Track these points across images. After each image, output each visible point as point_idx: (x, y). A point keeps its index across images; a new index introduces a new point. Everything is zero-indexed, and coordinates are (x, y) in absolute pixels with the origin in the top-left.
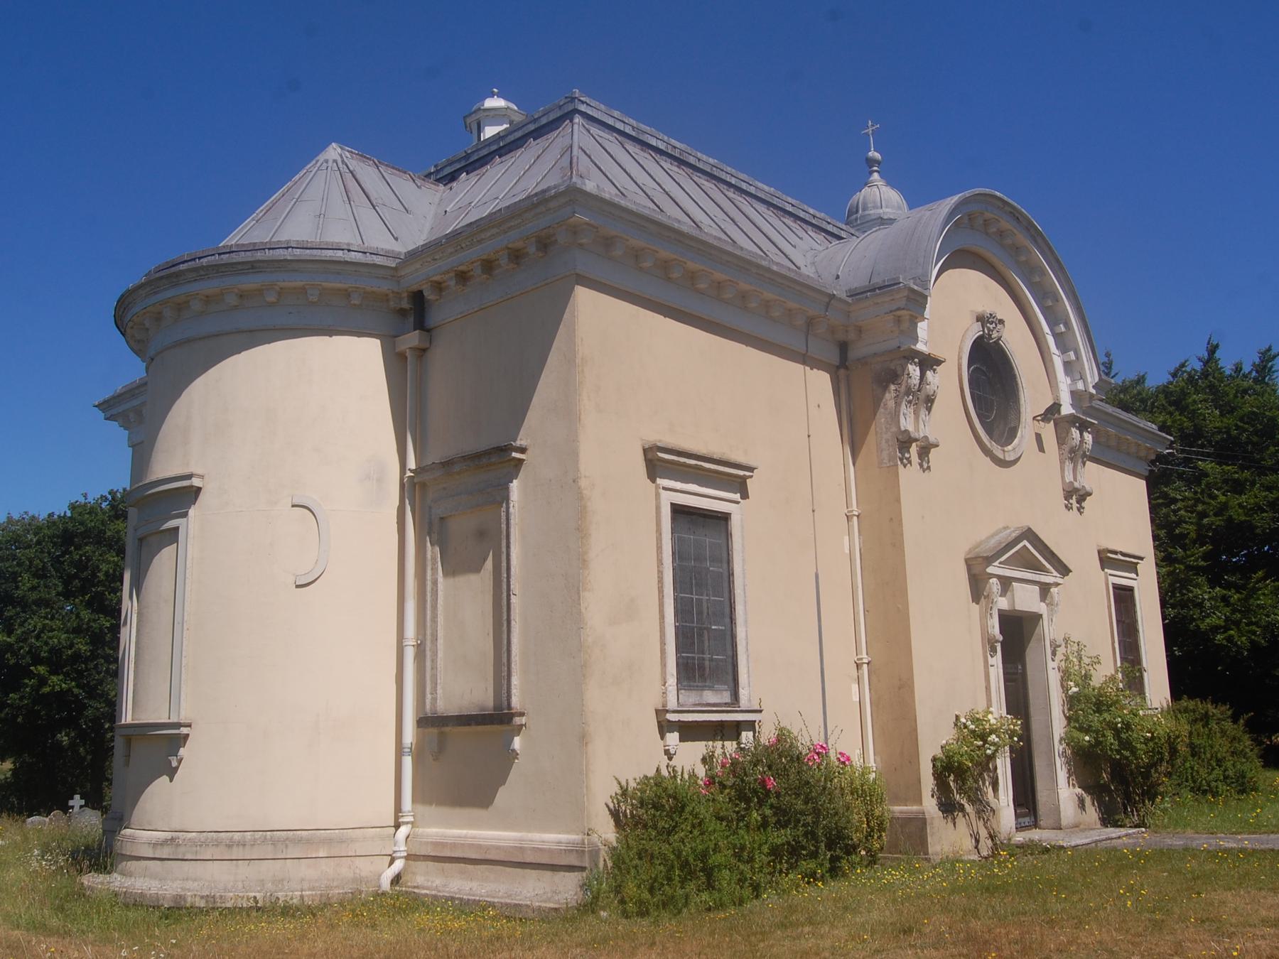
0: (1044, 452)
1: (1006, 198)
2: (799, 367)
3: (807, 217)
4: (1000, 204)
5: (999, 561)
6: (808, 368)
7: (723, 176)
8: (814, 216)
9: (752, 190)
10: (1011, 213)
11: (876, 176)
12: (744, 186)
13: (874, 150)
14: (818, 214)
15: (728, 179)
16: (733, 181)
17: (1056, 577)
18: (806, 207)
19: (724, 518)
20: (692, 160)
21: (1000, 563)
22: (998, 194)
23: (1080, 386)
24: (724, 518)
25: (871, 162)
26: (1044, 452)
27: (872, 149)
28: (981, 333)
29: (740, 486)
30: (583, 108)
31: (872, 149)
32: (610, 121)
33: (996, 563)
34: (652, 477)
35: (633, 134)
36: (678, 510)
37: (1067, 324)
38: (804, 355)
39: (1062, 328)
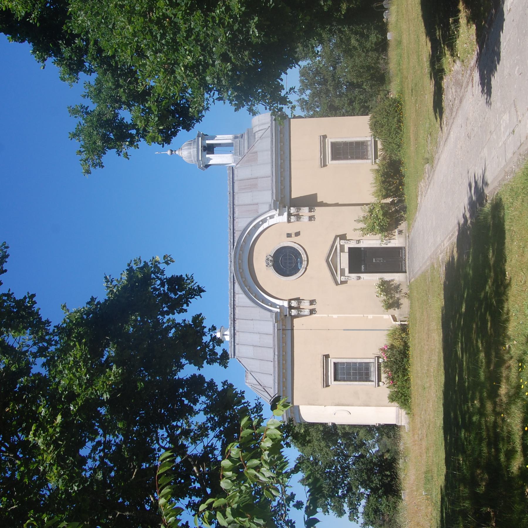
0: (300, 232)
2: (295, 331)
6: (294, 328)
7: (232, 304)
9: (232, 291)
11: (177, 152)
12: (232, 294)
15: (232, 301)
16: (232, 299)
19: (335, 363)
20: (232, 316)
23: (277, 215)
24: (335, 363)
25: (172, 154)
26: (300, 232)
29: (327, 357)
30: (233, 356)
32: (233, 346)
34: (329, 386)
35: (233, 338)
36: (335, 380)
37: (259, 222)
38: (291, 330)
39: (261, 223)
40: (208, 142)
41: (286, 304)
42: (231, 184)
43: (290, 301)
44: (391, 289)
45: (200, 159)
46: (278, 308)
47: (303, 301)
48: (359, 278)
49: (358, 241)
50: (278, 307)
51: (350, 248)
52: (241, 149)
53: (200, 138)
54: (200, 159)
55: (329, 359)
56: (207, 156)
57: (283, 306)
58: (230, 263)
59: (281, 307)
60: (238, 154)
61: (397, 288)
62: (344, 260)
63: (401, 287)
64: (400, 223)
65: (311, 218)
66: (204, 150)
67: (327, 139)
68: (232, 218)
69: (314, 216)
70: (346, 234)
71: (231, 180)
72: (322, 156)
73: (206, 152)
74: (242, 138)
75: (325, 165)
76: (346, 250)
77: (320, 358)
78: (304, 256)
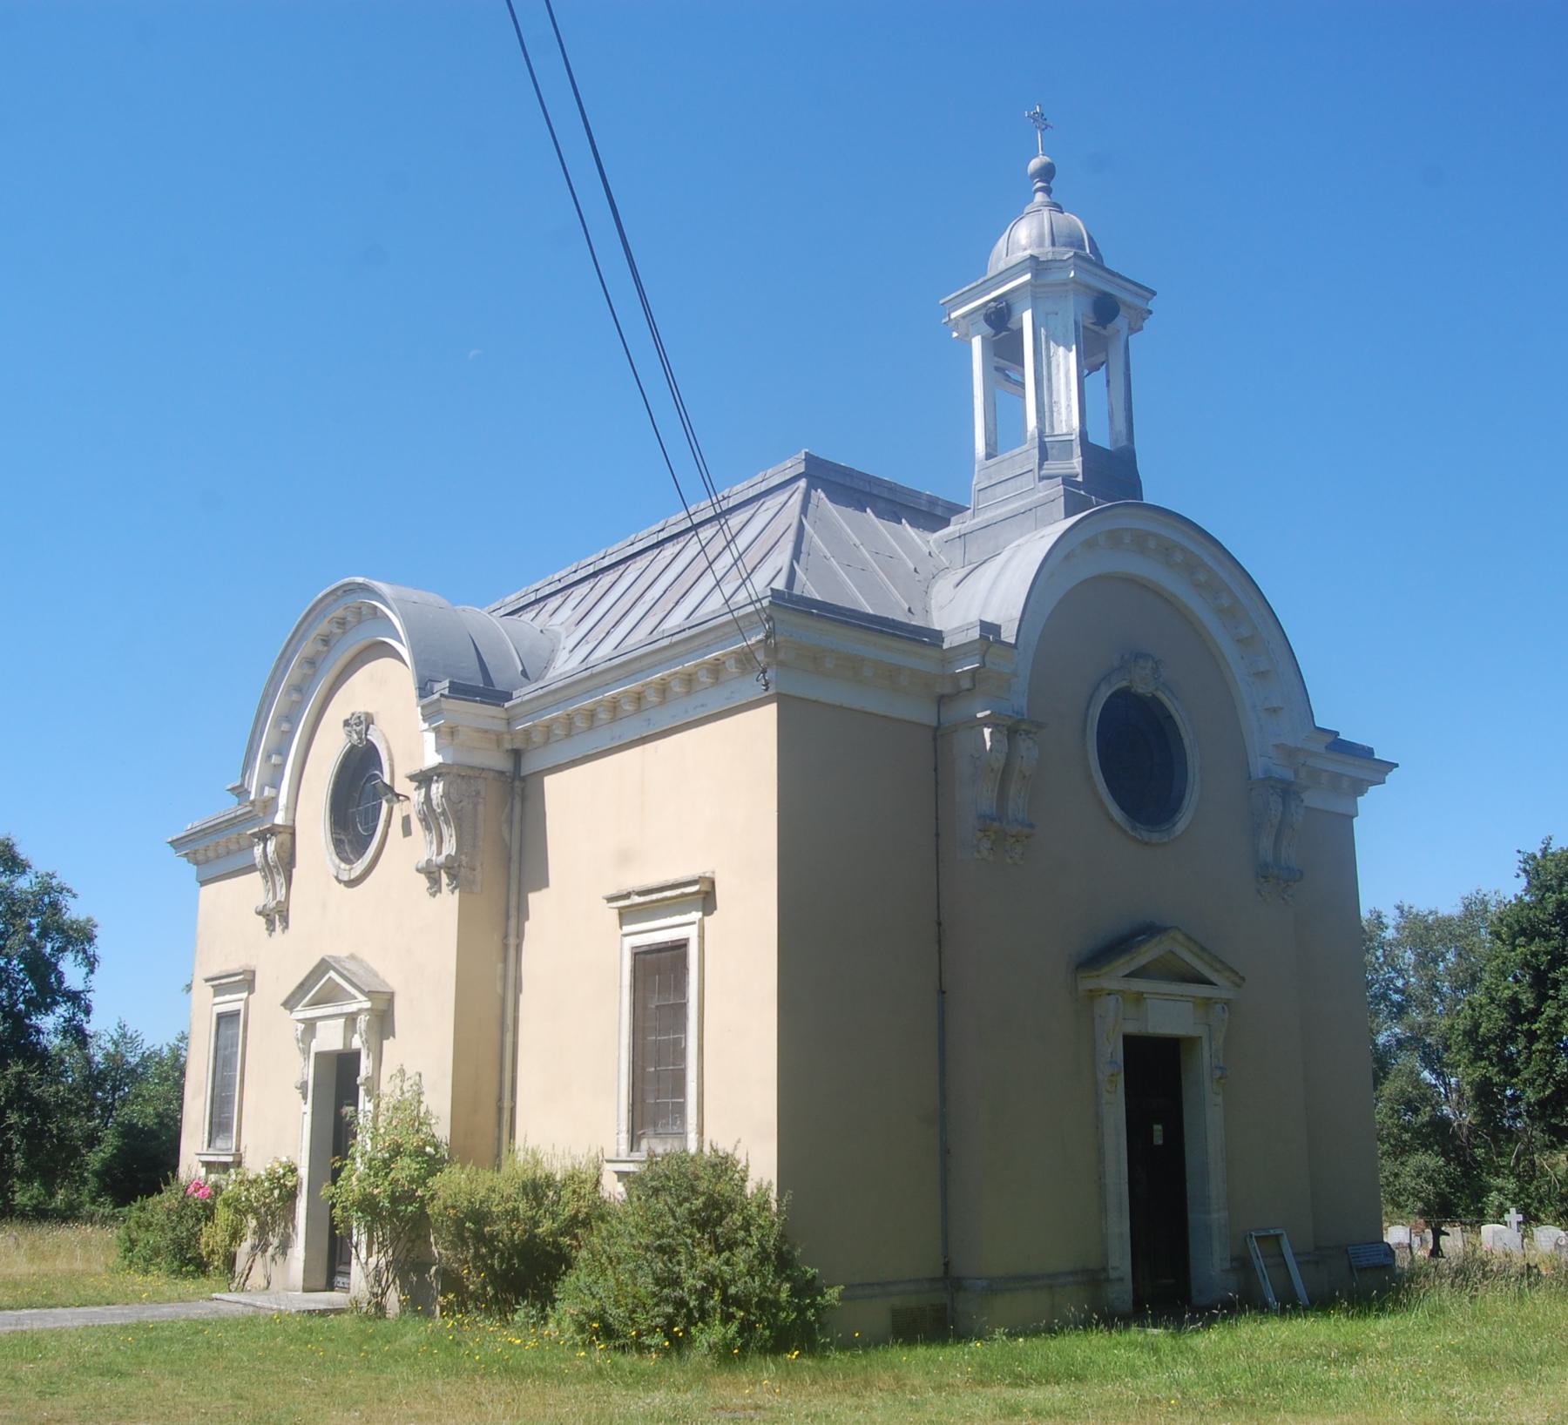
1: (328, 589)
3: (553, 588)
4: (333, 597)
5: (302, 1004)
8: (559, 580)
10: (345, 592)
13: (1043, 155)
14: (563, 573)
17: (360, 1002)
18: (550, 578)
21: (303, 1007)
22: (320, 596)
27: (1041, 152)
28: (349, 744)
31: (1041, 152)
33: (299, 1008)
40: (1027, 317)
41: (279, 819)
42: (752, 493)
43: (292, 831)
44: (286, 1227)
45: (953, 315)
46: (261, 790)
47: (283, 880)
48: (305, 1097)
49: (373, 1093)
50: (268, 792)
51: (357, 1054)
52: (999, 489)
53: (1028, 277)
54: (953, 315)
55: (244, 995)
56: (977, 343)
57: (277, 812)
58: (557, 577)
59: (270, 805)
60: (982, 486)
61: (285, 1246)
62: (330, 1038)
63: (279, 1259)
64: (398, 1282)
65: (431, 873)
66: (988, 319)
67: (696, 915)
68: (663, 535)
69: (440, 892)
70: (394, 1036)
71: (763, 487)
72: (637, 899)
73: (988, 330)
74: (1042, 478)
75: (626, 916)
76: (357, 1042)
77: (252, 963)
78: (359, 866)
